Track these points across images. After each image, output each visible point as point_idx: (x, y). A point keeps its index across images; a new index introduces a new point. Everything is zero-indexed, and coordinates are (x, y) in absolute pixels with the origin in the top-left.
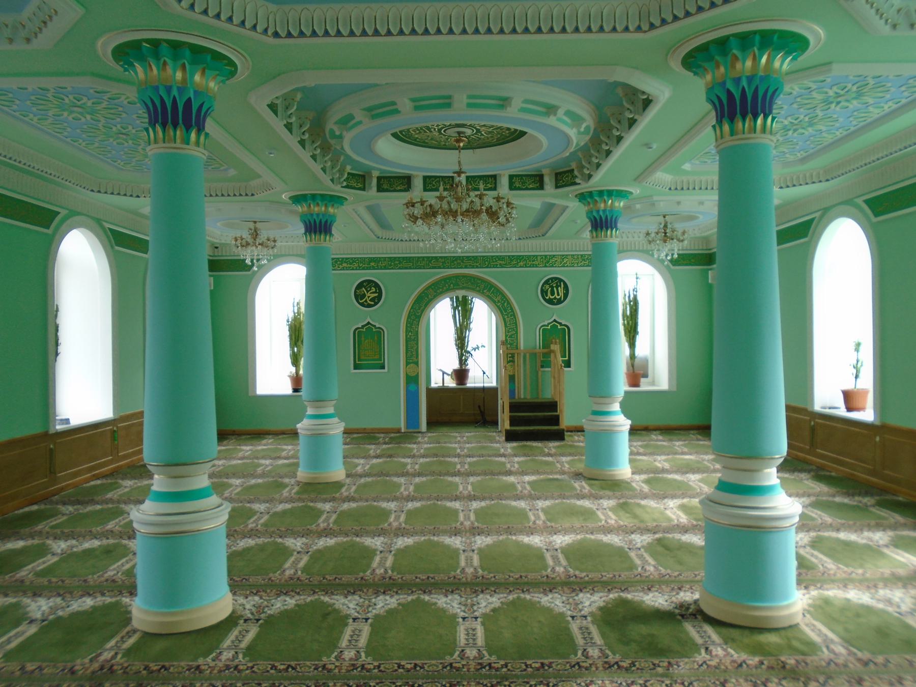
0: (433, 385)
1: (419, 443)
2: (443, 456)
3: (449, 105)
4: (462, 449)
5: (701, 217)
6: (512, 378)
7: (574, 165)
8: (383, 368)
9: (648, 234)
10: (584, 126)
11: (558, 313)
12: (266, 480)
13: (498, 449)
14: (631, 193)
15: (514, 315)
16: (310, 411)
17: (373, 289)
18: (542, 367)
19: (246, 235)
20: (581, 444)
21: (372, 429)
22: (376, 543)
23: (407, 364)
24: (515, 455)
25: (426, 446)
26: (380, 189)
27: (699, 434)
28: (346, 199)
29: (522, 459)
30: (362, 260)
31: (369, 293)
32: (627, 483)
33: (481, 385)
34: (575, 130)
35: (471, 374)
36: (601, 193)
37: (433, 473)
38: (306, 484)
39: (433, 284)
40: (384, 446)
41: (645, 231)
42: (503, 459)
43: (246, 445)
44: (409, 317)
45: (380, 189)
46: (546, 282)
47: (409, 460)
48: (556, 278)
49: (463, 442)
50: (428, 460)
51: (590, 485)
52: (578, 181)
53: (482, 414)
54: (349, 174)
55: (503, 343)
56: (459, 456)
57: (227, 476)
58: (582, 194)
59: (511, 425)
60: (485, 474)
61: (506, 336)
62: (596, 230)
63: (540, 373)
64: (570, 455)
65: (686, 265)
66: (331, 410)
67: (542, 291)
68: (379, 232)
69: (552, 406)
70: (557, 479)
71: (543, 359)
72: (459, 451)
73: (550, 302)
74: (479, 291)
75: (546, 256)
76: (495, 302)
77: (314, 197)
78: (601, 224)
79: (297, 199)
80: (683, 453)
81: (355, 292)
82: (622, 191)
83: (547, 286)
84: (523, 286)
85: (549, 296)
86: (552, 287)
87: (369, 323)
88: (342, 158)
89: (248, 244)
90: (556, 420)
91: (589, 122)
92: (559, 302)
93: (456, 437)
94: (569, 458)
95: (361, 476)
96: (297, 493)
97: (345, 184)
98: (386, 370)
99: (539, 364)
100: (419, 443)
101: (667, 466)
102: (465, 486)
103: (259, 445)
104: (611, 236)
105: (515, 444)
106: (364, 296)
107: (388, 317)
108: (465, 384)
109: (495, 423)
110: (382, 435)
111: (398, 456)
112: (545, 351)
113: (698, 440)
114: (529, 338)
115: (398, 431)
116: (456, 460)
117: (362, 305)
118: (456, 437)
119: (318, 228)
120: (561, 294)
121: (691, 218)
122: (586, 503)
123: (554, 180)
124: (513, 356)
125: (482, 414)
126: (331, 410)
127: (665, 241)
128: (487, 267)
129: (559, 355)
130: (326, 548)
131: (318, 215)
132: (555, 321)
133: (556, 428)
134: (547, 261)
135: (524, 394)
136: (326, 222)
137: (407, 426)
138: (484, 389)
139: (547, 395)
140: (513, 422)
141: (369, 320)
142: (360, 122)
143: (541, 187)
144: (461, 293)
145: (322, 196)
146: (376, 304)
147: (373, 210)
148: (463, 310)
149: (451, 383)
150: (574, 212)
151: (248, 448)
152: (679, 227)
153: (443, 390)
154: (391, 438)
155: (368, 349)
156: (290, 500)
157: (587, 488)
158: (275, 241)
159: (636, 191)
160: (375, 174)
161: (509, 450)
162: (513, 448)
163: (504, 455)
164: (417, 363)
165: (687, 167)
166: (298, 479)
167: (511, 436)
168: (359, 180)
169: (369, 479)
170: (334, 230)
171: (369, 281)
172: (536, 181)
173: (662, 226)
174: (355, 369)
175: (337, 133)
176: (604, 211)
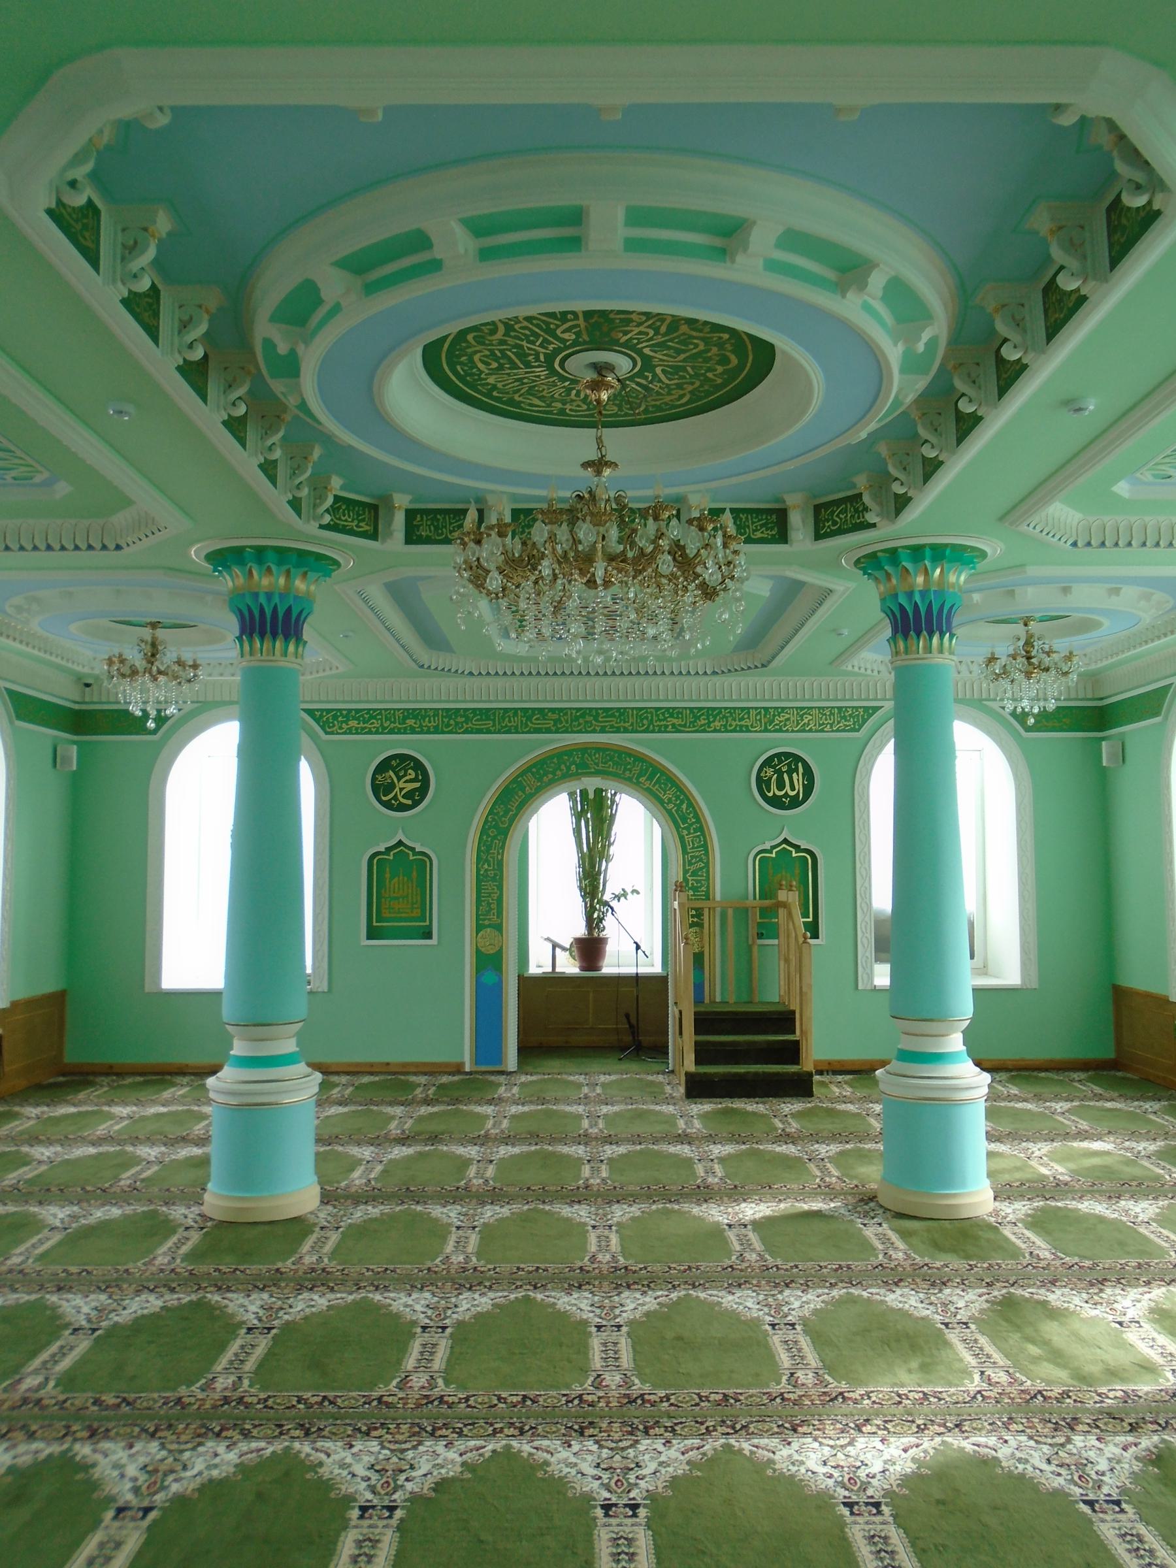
0: (533, 970)
1: (500, 1101)
2: (553, 1141)
3: (575, 243)
4: (593, 1117)
5: (1106, 622)
6: (698, 960)
7: (861, 482)
8: (428, 935)
9: (992, 659)
10: (926, 336)
11: (794, 826)
12: (128, 1210)
13: (670, 1120)
14: (983, 554)
15: (701, 829)
16: (239, 1048)
17: (412, 774)
18: (760, 936)
19: (136, 657)
20: (850, 1107)
21: (405, 1065)
22: (412, 1305)
24: (712, 1139)
25: (514, 1109)
26: (411, 538)
27: (1090, 1080)
28: (338, 564)
29: (729, 1149)
30: (389, 714)
31: (399, 782)
32: (994, 1229)
33: (631, 970)
34: (901, 347)
35: (610, 948)
36: (917, 552)
37: (527, 1194)
38: (224, 1225)
39: (534, 765)
40: (424, 1110)
41: (986, 652)
42: (685, 1150)
43: (125, 1103)
45: (411, 538)
46: (768, 762)
47: (472, 1151)
48: (788, 755)
49: (596, 1096)
50: (516, 1150)
51: (905, 1235)
52: (871, 517)
53: (634, 1029)
54: (337, 498)
55: (680, 887)
56: (584, 1139)
57: (135, 1141)
58: (873, 556)
59: (698, 1062)
60: (647, 1194)
61: (685, 872)
62: (906, 636)
63: (755, 949)
64: (834, 1137)
65: (1053, 730)
66: (290, 1046)
68: (425, 656)
69: (784, 1020)
70: (818, 1214)
71: (761, 918)
72: (585, 1123)
73: (776, 802)
74: (630, 779)
75: (766, 709)
76: (661, 802)
77: (260, 552)
78: (915, 623)
79: (222, 559)
80: (1083, 1135)
81: (374, 779)
82: (964, 548)
83: (770, 771)
84: (719, 769)
85: (774, 791)
86: (780, 773)
87: (400, 843)
88: (317, 453)
89: (134, 673)
90: (792, 1052)
91: (936, 331)
92: (795, 803)
93: (579, 1086)
94: (834, 1148)
95: (359, 1199)
96: (195, 1255)
97: (327, 519)
98: (434, 941)
99: (753, 931)
100: (500, 1101)
101: (1061, 1171)
102: (603, 1233)
103: (154, 1102)
104: (941, 651)
105: (707, 1106)
106: (392, 786)
107: (439, 830)
108: (598, 969)
109: (659, 1050)
110: (423, 1079)
111: (452, 1140)
112: (767, 902)
113: (1100, 1097)
114: (731, 877)
115: (458, 1069)
116: (580, 1151)
117: (387, 805)
118: (579, 1086)
119: (270, 624)
120: (799, 787)
121: (1086, 626)
122: (907, 1300)
123: (811, 521)
124: (699, 913)
125: (634, 1029)
126: (290, 1046)
127: (1028, 675)
128: (646, 731)
129: (797, 912)
130: (213, 1489)
131: (269, 596)
132: (785, 841)
133: (793, 1069)
134: (769, 718)
135: (723, 994)
136: (289, 611)
137: (477, 1060)
138: (637, 979)
139: (772, 993)
140: (703, 1054)
141: (400, 836)
142: (336, 309)
143: (782, 536)
144: (591, 783)
145: (281, 552)
146: (416, 804)
147: (403, 595)
148: (595, 818)
149: (569, 966)
150: (856, 600)
151: (124, 1111)
152: (1061, 645)
153: (553, 981)
154: (442, 1087)
155: (393, 894)
156: (166, 1282)
157: (900, 1251)
158: (195, 666)
159: (993, 547)
160: (402, 501)
161: (697, 1124)
162: (704, 1117)
163: (684, 1138)
164: (499, 928)
165: (1122, 488)
166: (205, 1209)
167: (697, 1088)
168: (362, 516)
169: (374, 1211)
170: (307, 632)
172: (772, 523)
173: (1021, 643)
174: (368, 938)
175: (282, 348)
176: (923, 594)
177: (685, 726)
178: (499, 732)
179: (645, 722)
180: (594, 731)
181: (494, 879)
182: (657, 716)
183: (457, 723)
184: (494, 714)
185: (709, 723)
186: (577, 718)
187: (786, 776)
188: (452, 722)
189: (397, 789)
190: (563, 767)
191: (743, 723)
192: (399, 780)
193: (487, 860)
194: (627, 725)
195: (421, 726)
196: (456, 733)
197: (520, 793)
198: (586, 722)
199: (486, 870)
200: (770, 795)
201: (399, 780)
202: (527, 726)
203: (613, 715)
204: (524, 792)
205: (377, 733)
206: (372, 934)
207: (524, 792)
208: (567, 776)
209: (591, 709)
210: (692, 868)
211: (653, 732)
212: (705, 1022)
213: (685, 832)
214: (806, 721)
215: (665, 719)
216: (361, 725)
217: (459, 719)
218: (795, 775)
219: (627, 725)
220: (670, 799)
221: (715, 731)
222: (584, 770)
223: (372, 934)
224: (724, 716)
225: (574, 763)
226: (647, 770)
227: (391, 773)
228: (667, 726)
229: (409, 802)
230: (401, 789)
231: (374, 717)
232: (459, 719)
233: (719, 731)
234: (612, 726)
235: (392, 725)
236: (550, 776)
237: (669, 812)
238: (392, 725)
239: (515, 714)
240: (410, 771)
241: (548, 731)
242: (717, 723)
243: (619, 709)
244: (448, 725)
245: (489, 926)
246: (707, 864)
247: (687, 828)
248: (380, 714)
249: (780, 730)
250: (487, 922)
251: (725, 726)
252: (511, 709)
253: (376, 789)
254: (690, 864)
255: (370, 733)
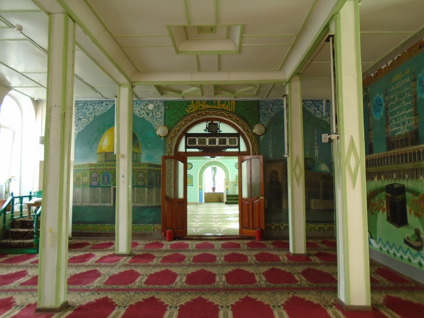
6: (227, 189)
53: (220, 200)
115: (197, 203)
125: (220, 200)
135: (230, 193)
144: (214, 166)
149: (211, 191)
164: (202, 185)
167: (227, 203)
208: (210, 165)
212: (228, 196)
222: (213, 164)
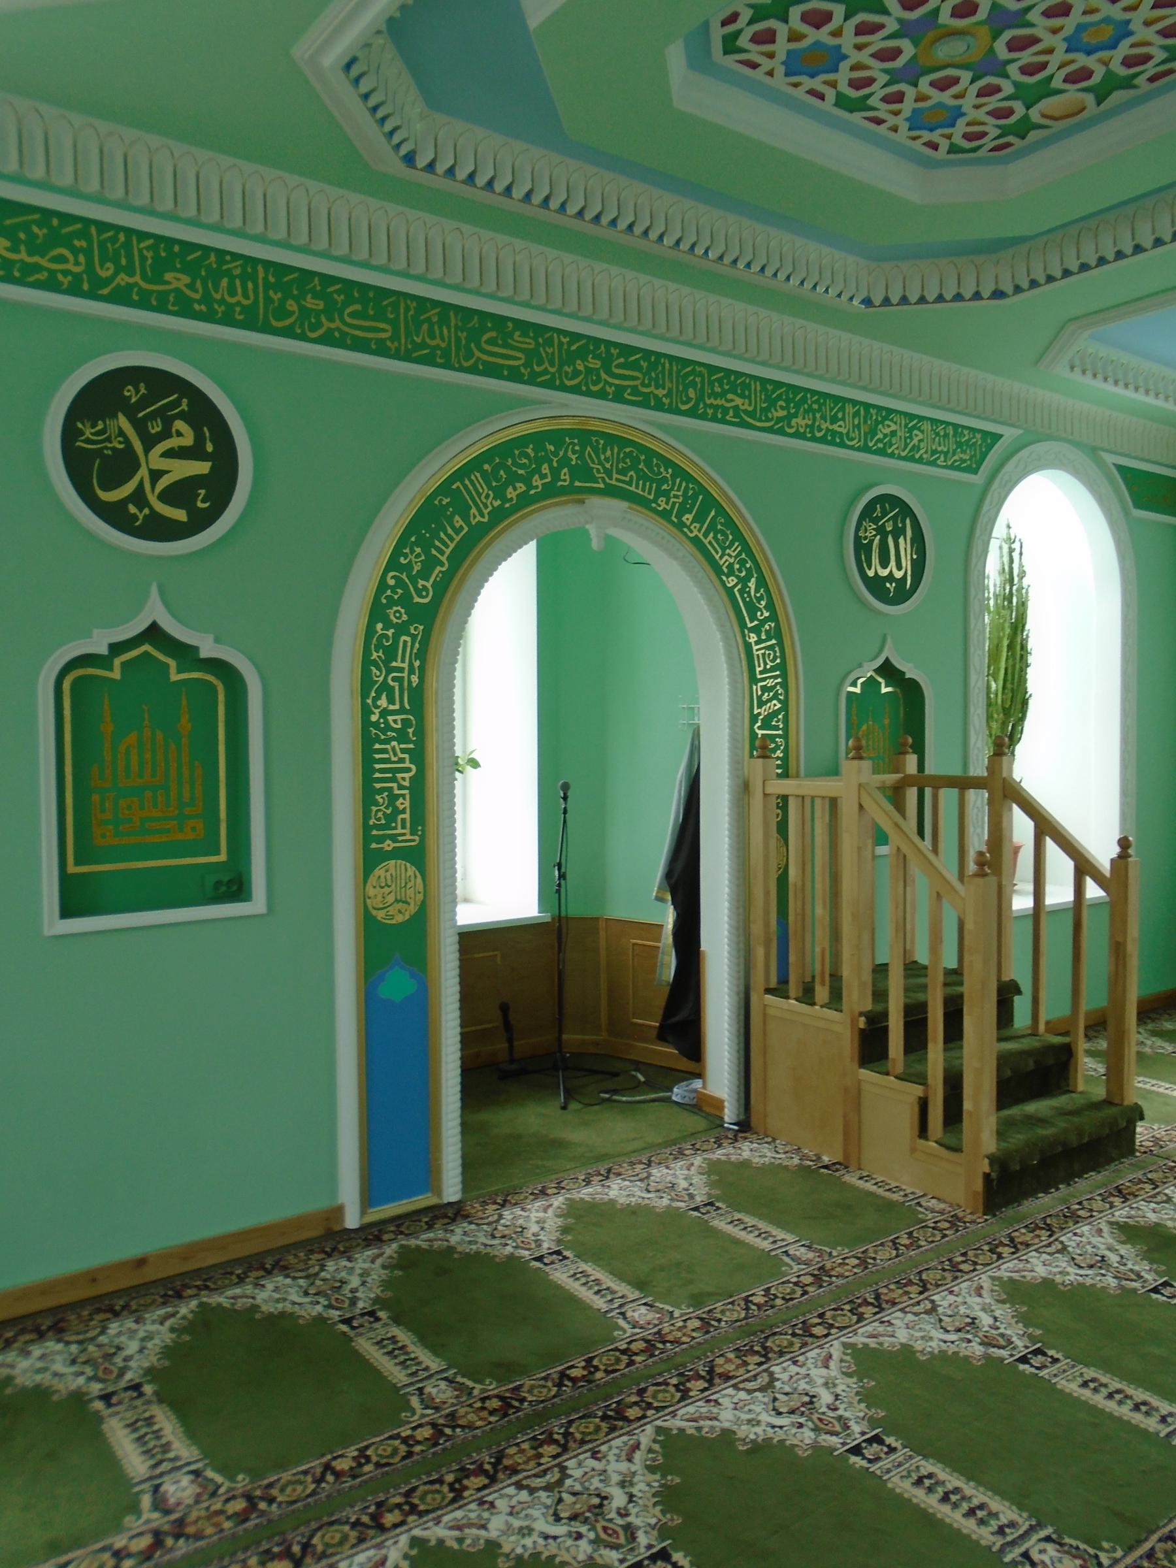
8: (234, 887)
17: (185, 435)
23: (370, 860)
30: (115, 242)
44: (377, 612)
67: (857, 539)
74: (665, 515)
81: (69, 434)
87: (153, 633)
98: (257, 904)
106: (121, 465)
117: (115, 516)
120: (906, 563)
128: (692, 413)
134: (870, 425)
141: (156, 612)
146: (200, 522)
164: (418, 856)
171: (161, 382)
174: (67, 912)
177: (751, 414)
178: (407, 358)
179: (692, 393)
180: (602, 395)
181: (402, 737)
182: (711, 383)
183: (305, 313)
184: (395, 307)
185: (789, 417)
186: (571, 358)
187: (890, 540)
188: (291, 305)
189: (143, 472)
190: (545, 469)
191: (835, 427)
192: (147, 451)
193: (385, 688)
194: (661, 392)
195: (207, 299)
196: (303, 338)
197: (458, 521)
198: (589, 371)
199: (385, 713)
200: (871, 573)
201: (148, 446)
202: (469, 355)
203: (635, 366)
204: (466, 518)
205: (74, 290)
206: (75, 901)
207: (466, 518)
209: (597, 341)
210: (764, 711)
211: (703, 417)
213: (753, 638)
214: (915, 441)
215: (723, 395)
216: (23, 255)
217: (310, 302)
218: (901, 540)
219: (661, 392)
220: (730, 566)
221: (797, 435)
222: (578, 485)
223: (75, 901)
224: (810, 409)
225: (564, 462)
226: (695, 497)
227: (123, 422)
228: (725, 411)
229: (180, 515)
230: (156, 475)
231: (67, 242)
232: (310, 302)
233: (802, 436)
234: (635, 391)
235: (123, 279)
236: (521, 487)
237: (729, 591)
238: (123, 279)
239: (444, 320)
240: (179, 425)
241: (514, 376)
242: (799, 420)
243: (647, 353)
244: (282, 313)
245: (396, 854)
246: (785, 704)
247: (756, 630)
248: (84, 234)
249: (882, 452)
250: (388, 845)
251: (811, 427)
252: (436, 303)
253: (78, 464)
254: (761, 704)
255: (52, 285)
